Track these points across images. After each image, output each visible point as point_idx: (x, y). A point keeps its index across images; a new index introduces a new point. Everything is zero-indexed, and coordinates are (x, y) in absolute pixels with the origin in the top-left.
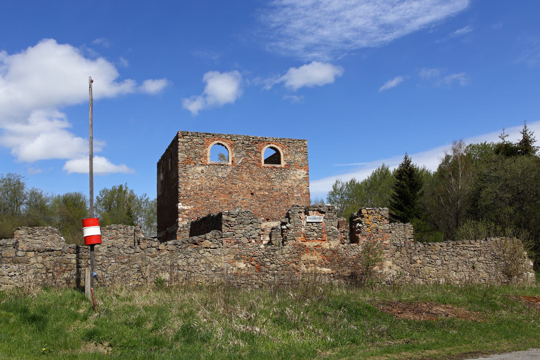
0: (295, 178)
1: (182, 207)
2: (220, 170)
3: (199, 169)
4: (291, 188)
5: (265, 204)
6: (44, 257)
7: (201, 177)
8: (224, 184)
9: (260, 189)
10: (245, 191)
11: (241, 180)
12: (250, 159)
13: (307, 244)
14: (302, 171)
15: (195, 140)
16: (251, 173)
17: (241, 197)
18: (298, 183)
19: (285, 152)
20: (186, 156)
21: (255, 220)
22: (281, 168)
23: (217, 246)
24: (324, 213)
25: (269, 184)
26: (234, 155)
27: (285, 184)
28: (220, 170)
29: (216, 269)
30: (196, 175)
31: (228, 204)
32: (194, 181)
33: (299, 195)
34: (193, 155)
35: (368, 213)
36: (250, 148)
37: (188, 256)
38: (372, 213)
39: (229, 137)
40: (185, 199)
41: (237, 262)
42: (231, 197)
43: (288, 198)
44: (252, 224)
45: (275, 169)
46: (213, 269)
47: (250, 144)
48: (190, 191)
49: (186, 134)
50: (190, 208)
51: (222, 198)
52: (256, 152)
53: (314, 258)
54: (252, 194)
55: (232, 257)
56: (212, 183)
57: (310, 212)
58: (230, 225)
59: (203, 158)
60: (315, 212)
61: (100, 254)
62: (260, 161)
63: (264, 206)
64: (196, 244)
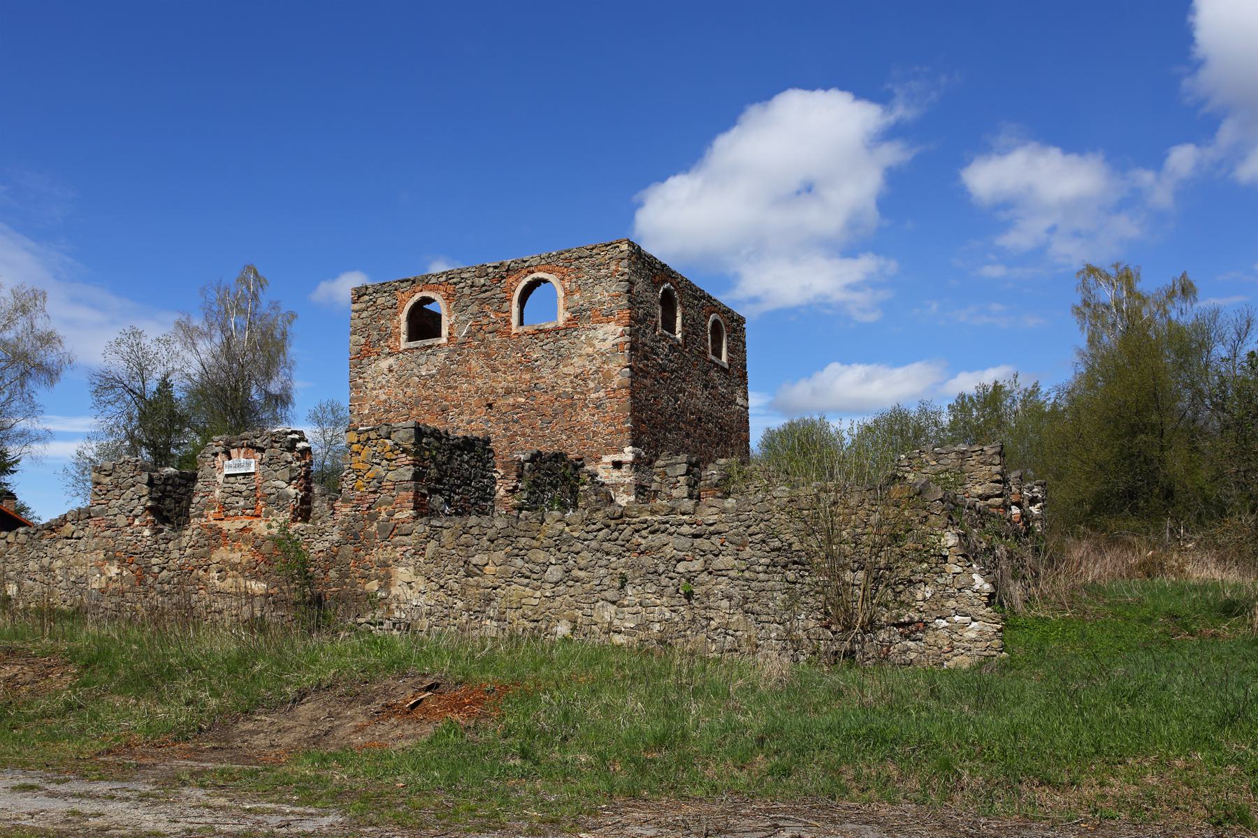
0: (590, 350)
2: (423, 359)
3: (384, 364)
5: (517, 426)
9: (508, 392)
12: (485, 321)
16: (488, 356)
17: (465, 418)
18: (598, 363)
19: (567, 285)
22: (557, 330)
25: (527, 377)
26: (453, 318)
33: (602, 394)
36: (488, 294)
43: (571, 406)
45: (542, 336)
47: (488, 283)
48: (368, 416)
52: (503, 300)
53: (236, 557)
54: (490, 406)
55: (102, 556)
56: (409, 391)
57: (234, 452)
60: (243, 451)
62: (508, 323)
63: (516, 434)
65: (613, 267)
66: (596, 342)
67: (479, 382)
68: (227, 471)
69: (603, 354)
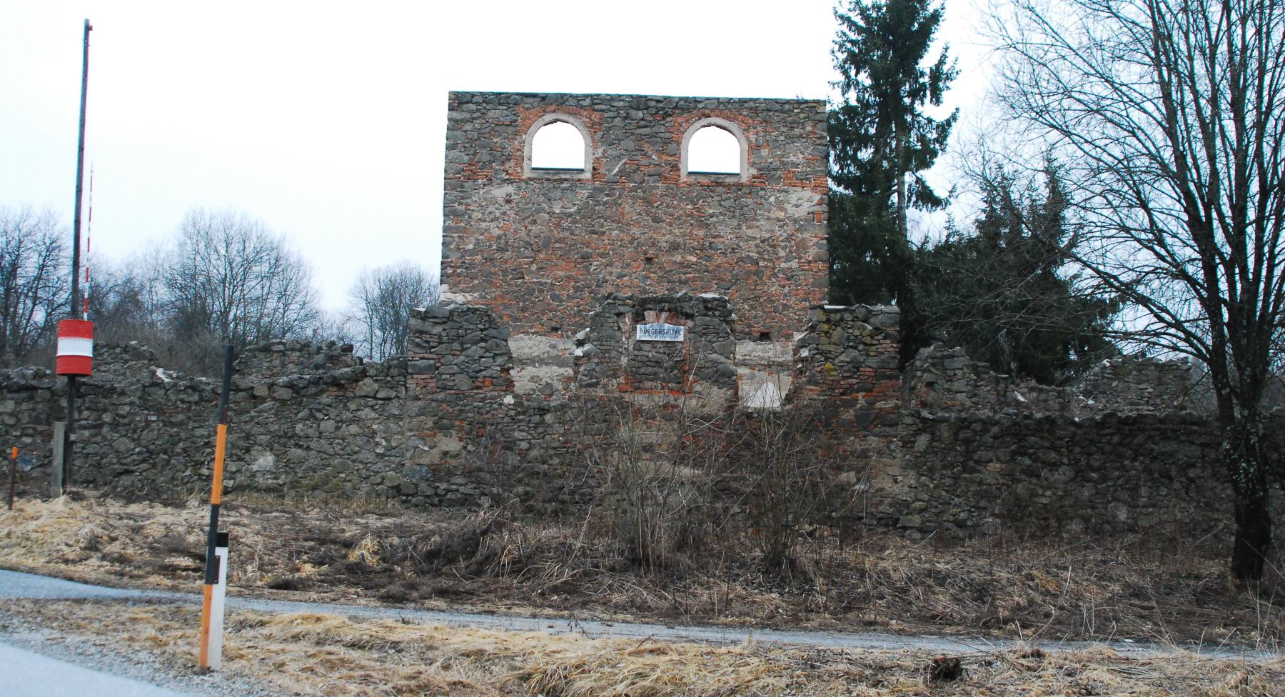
0: (781, 215)
1: (450, 295)
2: (558, 193)
3: (499, 192)
4: (770, 243)
6: (18, 403)
7: (504, 214)
8: (567, 234)
9: (674, 247)
10: (628, 252)
11: (619, 221)
12: (645, 162)
13: (640, 399)
14: (807, 193)
15: (491, 114)
16: (649, 203)
18: (790, 229)
19: (753, 138)
20: (466, 159)
21: (494, 332)
23: (393, 394)
24: (689, 316)
25: (701, 233)
26: (600, 151)
27: (749, 232)
28: (558, 193)
29: (386, 449)
30: (491, 209)
31: (577, 289)
32: (483, 225)
33: (794, 264)
34: (484, 155)
35: (828, 321)
36: (647, 130)
37: (319, 415)
38: (842, 319)
39: (588, 102)
40: (459, 275)
41: (440, 436)
42: (587, 268)
43: (757, 273)
44: (486, 341)
45: (720, 189)
46: (380, 450)
49: (468, 98)
50: (470, 298)
51: (561, 273)
52: (668, 141)
53: (652, 437)
54: (649, 260)
55: (430, 424)
57: (650, 315)
58: (428, 342)
59: (512, 163)
61: (128, 400)
64: (340, 386)
65: (809, 129)
66: (788, 207)
67: (634, 230)
68: (640, 336)
69: (795, 221)
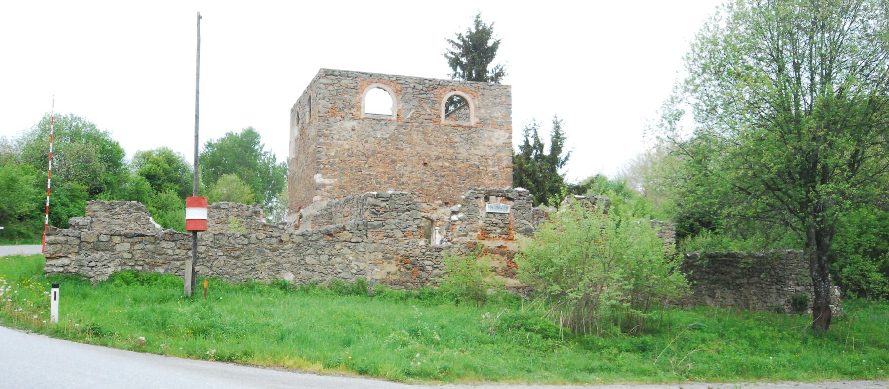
0: (490, 143)
1: (322, 180)
2: (379, 127)
3: (349, 125)
5: (443, 179)
8: (384, 149)
9: (438, 158)
10: (415, 159)
11: (411, 143)
12: (423, 112)
13: (487, 243)
15: (343, 82)
16: (425, 134)
17: (409, 169)
19: (477, 103)
21: (414, 206)
22: (470, 128)
23: (360, 240)
27: (475, 152)
30: (344, 133)
31: (389, 178)
32: (340, 142)
33: (496, 169)
37: (320, 252)
39: (394, 79)
41: (386, 263)
45: (461, 129)
46: (354, 271)
47: (425, 89)
48: (334, 157)
51: (381, 170)
52: (435, 102)
54: (425, 164)
55: (380, 257)
56: (367, 145)
57: (492, 198)
59: (355, 109)
60: (499, 199)
61: (204, 243)
62: (438, 116)
63: (442, 184)
64: (331, 235)
65: (503, 99)
66: (494, 139)
67: (418, 148)
68: (488, 210)
69: (497, 147)
